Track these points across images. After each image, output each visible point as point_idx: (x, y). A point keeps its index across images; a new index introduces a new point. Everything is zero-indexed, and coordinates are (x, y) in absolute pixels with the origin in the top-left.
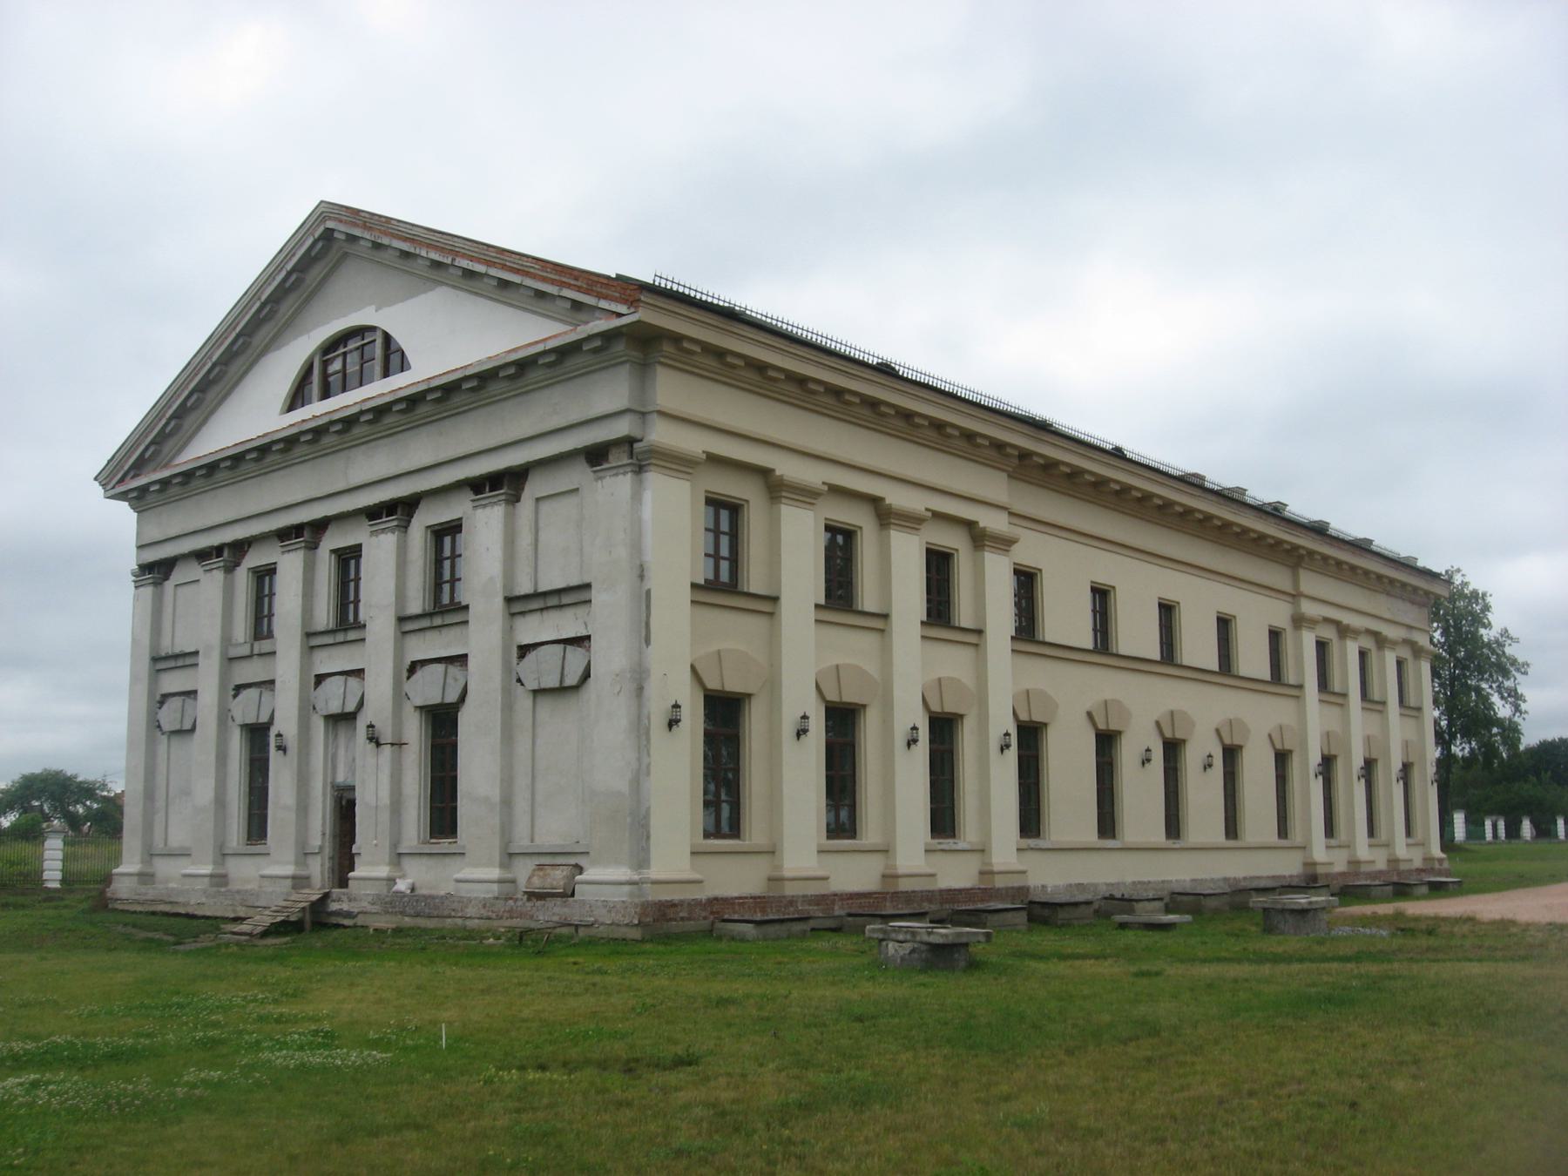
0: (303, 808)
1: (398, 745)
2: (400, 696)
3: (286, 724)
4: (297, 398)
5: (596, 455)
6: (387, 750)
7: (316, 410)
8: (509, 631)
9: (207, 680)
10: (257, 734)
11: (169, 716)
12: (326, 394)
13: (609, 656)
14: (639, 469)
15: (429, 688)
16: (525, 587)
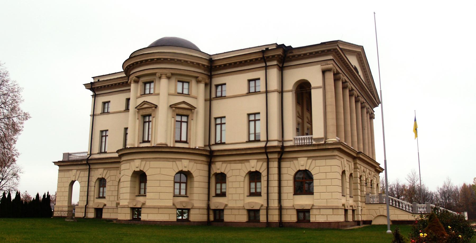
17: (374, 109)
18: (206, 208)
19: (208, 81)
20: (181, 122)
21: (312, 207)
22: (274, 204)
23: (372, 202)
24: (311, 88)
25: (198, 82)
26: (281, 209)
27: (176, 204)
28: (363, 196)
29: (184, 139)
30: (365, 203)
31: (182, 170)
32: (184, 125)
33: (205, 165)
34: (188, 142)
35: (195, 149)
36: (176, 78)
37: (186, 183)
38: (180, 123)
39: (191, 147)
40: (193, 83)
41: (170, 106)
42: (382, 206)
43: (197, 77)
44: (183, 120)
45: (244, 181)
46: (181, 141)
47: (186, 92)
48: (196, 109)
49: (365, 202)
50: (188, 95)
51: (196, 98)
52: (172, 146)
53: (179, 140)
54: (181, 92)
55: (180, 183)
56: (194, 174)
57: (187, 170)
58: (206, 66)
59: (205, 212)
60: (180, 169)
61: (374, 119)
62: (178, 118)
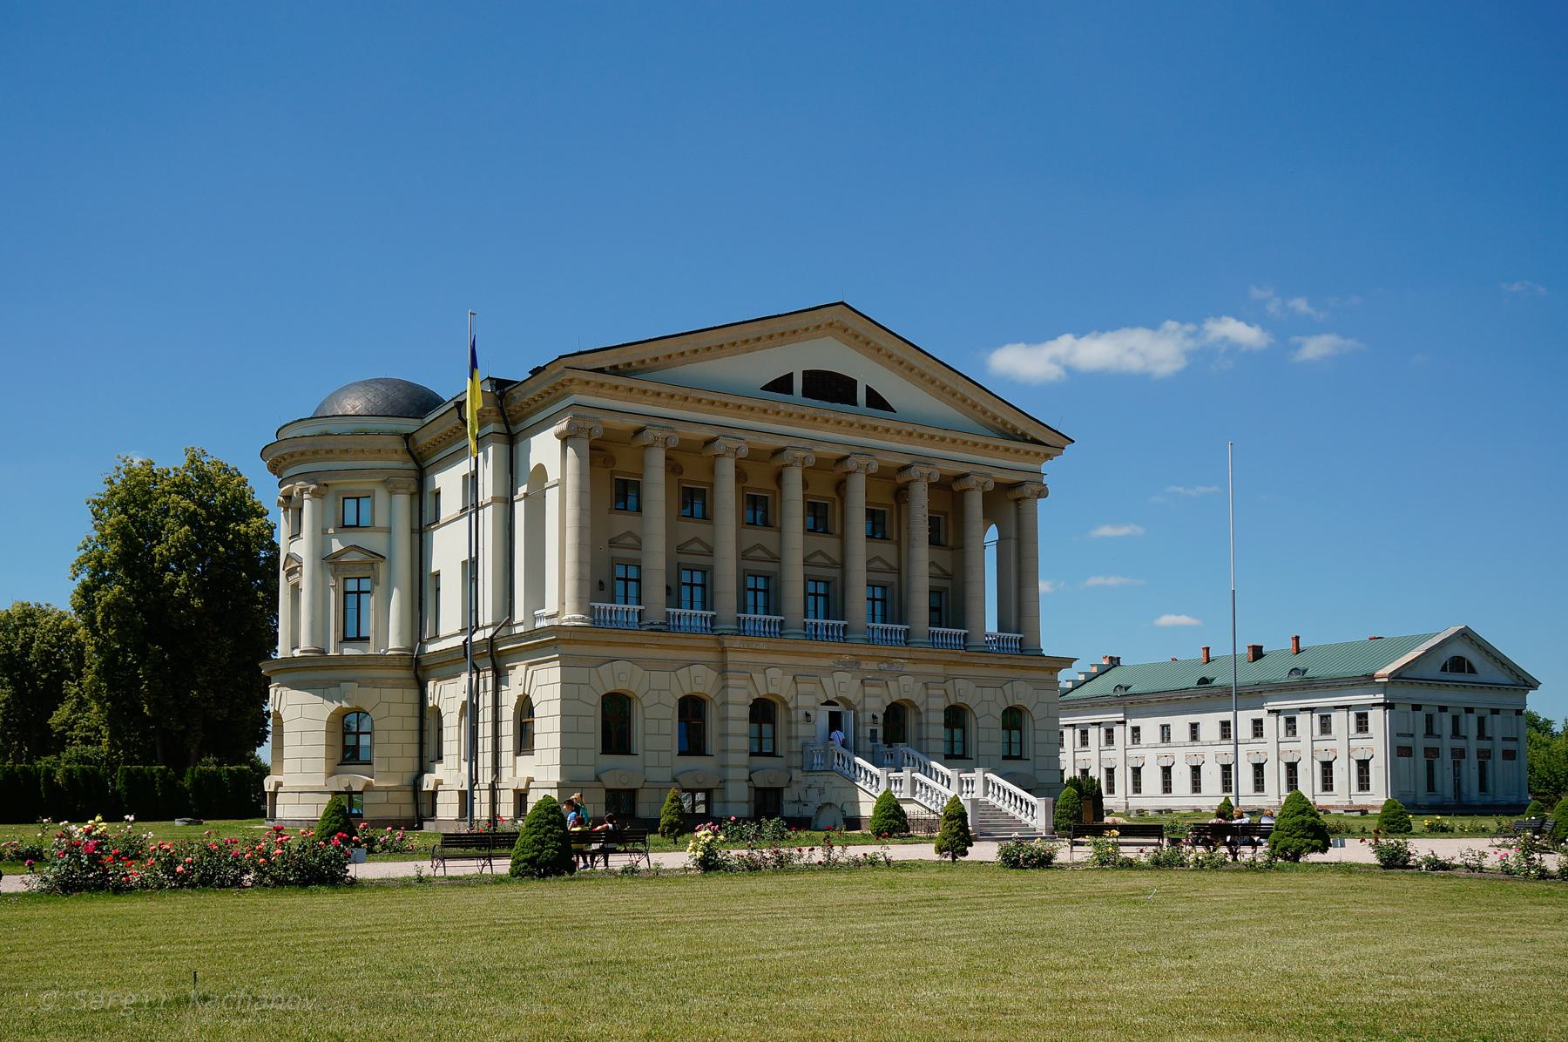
17: (1046, 467)
18: (410, 788)
19: (413, 488)
20: (359, 593)
21: (528, 784)
22: (486, 777)
23: (814, 768)
24: (546, 485)
25: (392, 491)
26: (494, 790)
28: (794, 749)
30: (800, 771)
33: (412, 690)
40: (381, 496)
42: (831, 779)
45: (460, 726)
49: (802, 768)
58: (400, 452)
59: (408, 797)
61: (1043, 493)
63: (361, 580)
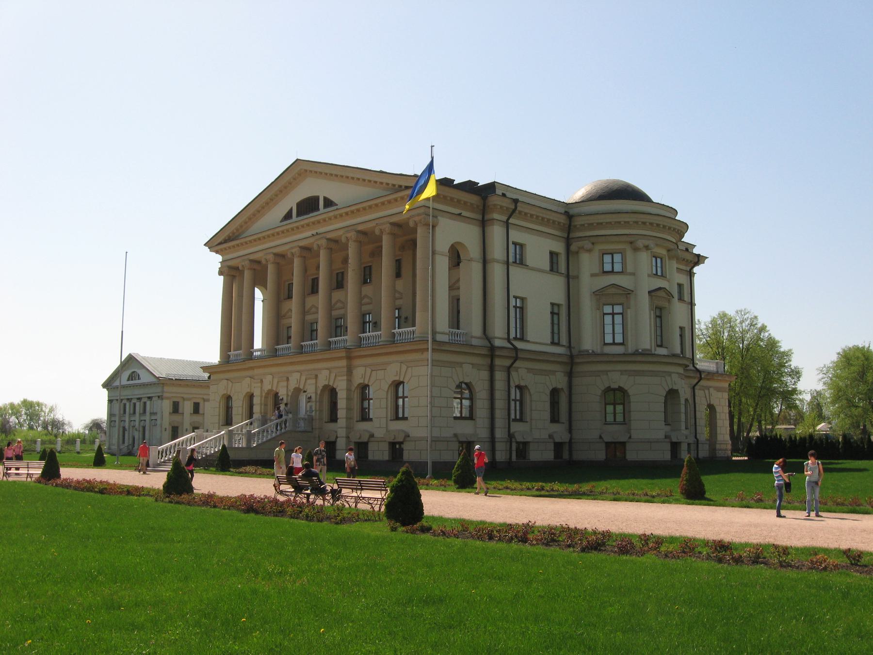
0: (129, 439)
1: (139, 431)
2: (139, 424)
3: (127, 427)
4: (128, 380)
5: (159, 397)
6: (138, 432)
7: (131, 382)
8: (150, 417)
9: (117, 419)
10: (124, 429)
11: (112, 424)
12: (132, 380)
13: (159, 422)
14: (162, 399)
15: (142, 423)
16: (152, 412)
20: (613, 314)
25: (636, 249)
27: (603, 436)
29: (619, 339)
31: (610, 387)
32: (618, 319)
34: (625, 343)
35: (636, 353)
36: (599, 250)
37: (624, 404)
38: (611, 316)
39: (630, 351)
41: (593, 293)
43: (631, 243)
44: (614, 312)
46: (614, 344)
47: (618, 268)
48: (634, 292)
50: (622, 273)
51: (633, 274)
52: (599, 351)
53: (611, 341)
54: (610, 269)
55: (614, 404)
56: (631, 392)
57: (617, 387)
60: (607, 386)
62: (608, 309)
63: (614, 306)
